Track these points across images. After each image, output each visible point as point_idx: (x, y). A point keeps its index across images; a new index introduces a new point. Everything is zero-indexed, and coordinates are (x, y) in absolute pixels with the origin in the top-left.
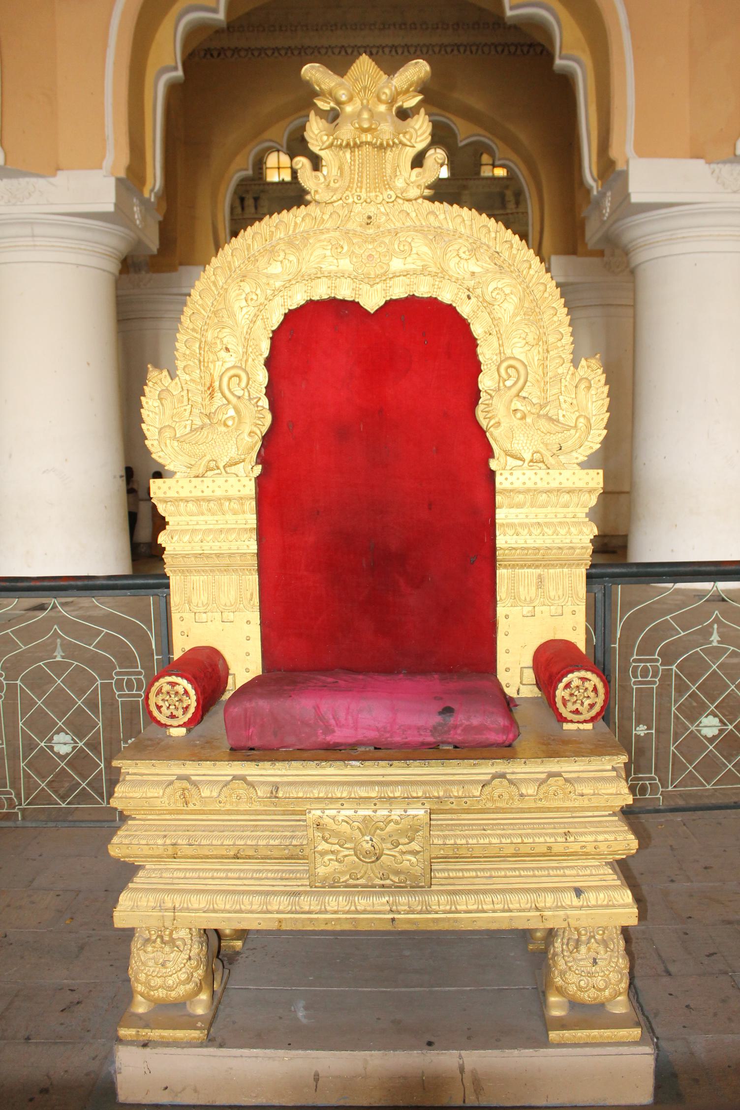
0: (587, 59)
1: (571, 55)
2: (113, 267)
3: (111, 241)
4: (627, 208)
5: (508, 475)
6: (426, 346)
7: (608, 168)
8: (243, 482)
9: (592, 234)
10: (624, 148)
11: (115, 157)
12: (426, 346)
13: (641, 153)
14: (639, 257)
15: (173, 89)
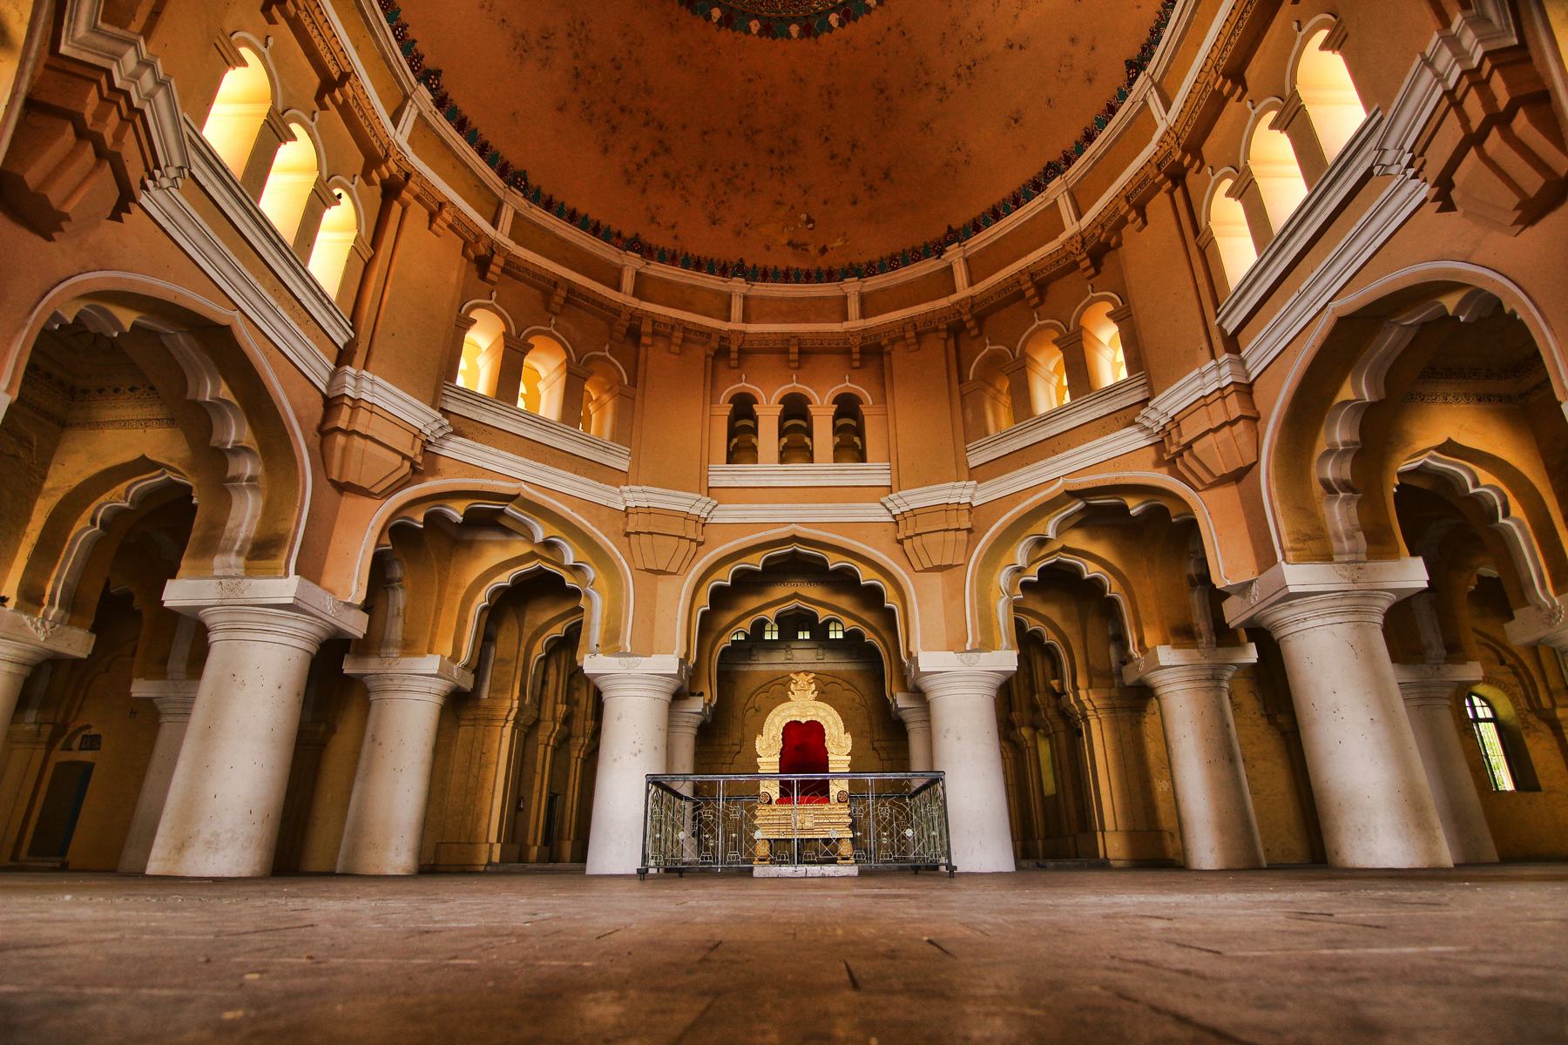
0: (899, 604)
1: (891, 600)
2: (669, 698)
3: (672, 686)
4: (919, 673)
5: (831, 757)
6: (815, 729)
7: (909, 654)
8: (777, 758)
9: (910, 686)
10: (916, 646)
11: (679, 650)
12: (815, 729)
13: (926, 648)
14: (930, 696)
15: (704, 614)
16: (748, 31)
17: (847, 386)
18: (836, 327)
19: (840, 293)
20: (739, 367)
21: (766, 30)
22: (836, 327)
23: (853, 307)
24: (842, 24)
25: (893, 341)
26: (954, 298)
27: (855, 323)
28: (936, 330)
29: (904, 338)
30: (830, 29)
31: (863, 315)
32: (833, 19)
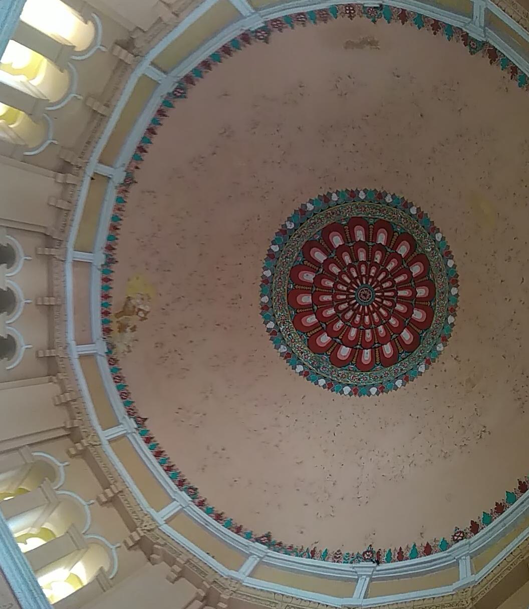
16: (265, 269)
17: (22, 347)
18: (71, 336)
19: (95, 340)
20: (37, 254)
21: (266, 281)
22: (71, 336)
23: (87, 349)
24: (268, 330)
25: (61, 382)
26: (98, 428)
27: (75, 351)
28: (73, 418)
29: (64, 392)
30: (266, 323)
31: (81, 357)
32: (271, 325)
